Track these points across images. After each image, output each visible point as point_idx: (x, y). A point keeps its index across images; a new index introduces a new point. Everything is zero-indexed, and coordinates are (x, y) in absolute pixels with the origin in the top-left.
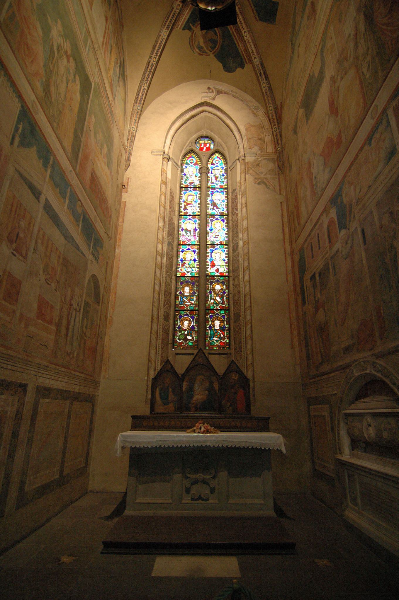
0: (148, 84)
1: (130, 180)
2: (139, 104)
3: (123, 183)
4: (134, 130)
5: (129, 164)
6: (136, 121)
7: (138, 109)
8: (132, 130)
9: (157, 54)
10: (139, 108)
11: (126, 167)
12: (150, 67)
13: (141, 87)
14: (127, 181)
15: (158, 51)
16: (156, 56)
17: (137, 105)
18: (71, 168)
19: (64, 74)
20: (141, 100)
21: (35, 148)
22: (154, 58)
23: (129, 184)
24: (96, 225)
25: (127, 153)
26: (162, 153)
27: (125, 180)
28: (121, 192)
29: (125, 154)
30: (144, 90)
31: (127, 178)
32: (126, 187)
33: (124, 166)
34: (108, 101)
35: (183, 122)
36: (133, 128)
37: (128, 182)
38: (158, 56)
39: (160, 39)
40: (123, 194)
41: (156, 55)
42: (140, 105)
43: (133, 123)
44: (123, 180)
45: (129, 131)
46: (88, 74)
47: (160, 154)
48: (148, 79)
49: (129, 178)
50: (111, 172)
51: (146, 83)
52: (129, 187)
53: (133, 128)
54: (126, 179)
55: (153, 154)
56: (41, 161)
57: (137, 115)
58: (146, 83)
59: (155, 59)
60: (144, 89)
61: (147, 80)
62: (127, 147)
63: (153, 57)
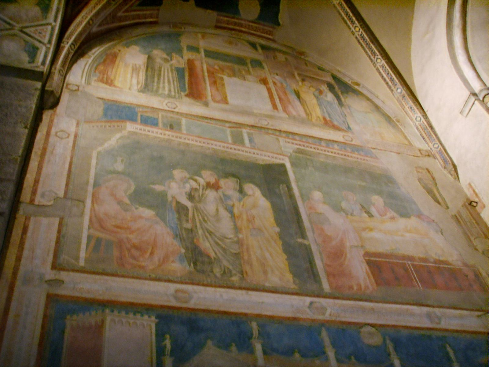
0: (380, 57)
1: (473, 185)
2: (395, 87)
3: (468, 199)
4: (421, 119)
5: (452, 167)
6: (411, 108)
7: (401, 93)
8: (417, 123)
9: (352, 21)
10: (399, 90)
11: (452, 175)
12: (361, 41)
13: (378, 70)
14: (471, 190)
15: (350, 19)
16: (354, 25)
17: (395, 90)
18: (308, 300)
19: (217, 210)
20: (392, 80)
21: (210, 343)
22: (355, 29)
23: (477, 191)
24: (444, 324)
25: (438, 156)
26: (473, 99)
27: (469, 193)
28: (478, 214)
29: (437, 161)
30: (383, 67)
31: (468, 186)
32: (476, 200)
33: (450, 176)
34: (336, 146)
35: (461, 26)
36: (416, 119)
37: (474, 191)
38: (356, 22)
39: (338, 7)
40: (482, 215)
41: (353, 24)
42: (397, 86)
43: (411, 114)
44: (466, 195)
45: (417, 128)
46: (268, 163)
47: (471, 104)
48: (374, 53)
49: (470, 184)
50: (420, 215)
51: (377, 58)
52: (480, 196)
53: (416, 119)
54: (468, 189)
55: (465, 115)
56: (234, 348)
57: (406, 99)
58: (377, 58)
59: (357, 29)
60: (382, 66)
61: (375, 55)
62: (431, 149)
63: (353, 29)
